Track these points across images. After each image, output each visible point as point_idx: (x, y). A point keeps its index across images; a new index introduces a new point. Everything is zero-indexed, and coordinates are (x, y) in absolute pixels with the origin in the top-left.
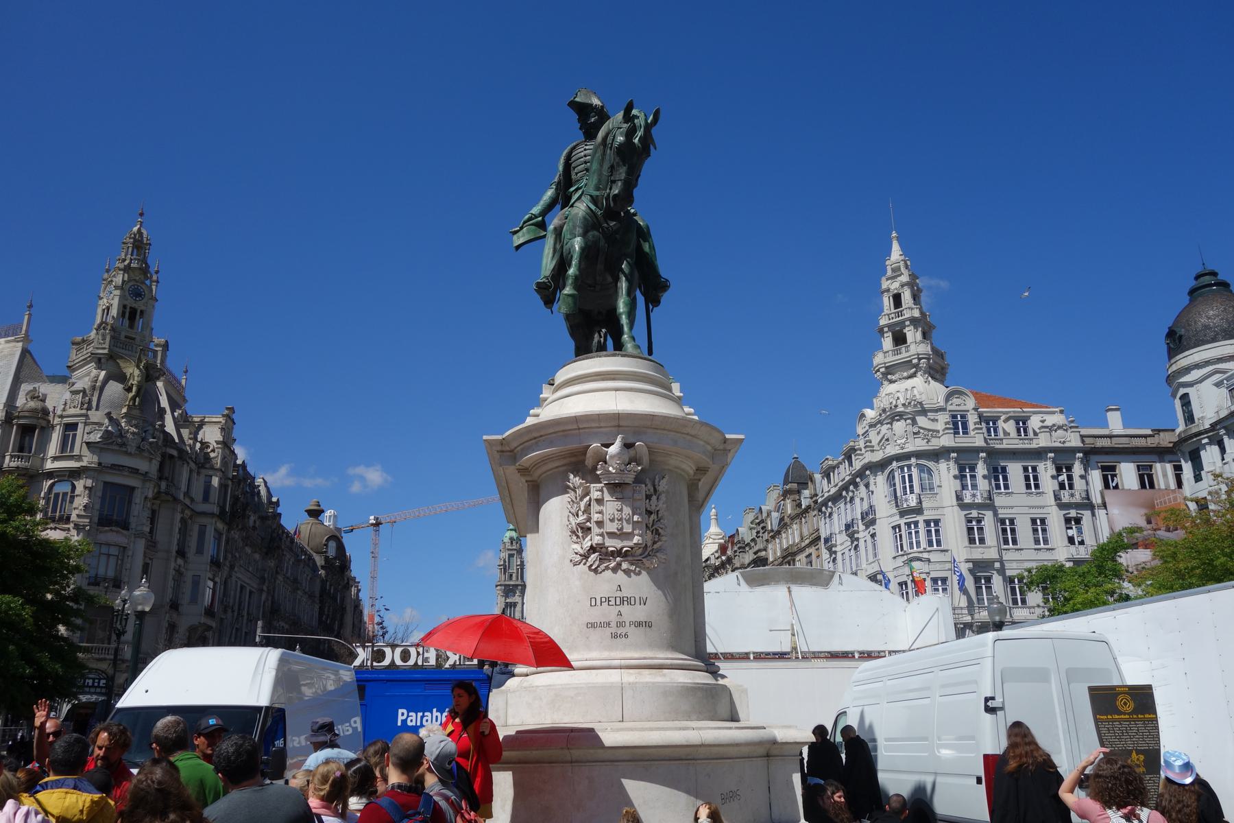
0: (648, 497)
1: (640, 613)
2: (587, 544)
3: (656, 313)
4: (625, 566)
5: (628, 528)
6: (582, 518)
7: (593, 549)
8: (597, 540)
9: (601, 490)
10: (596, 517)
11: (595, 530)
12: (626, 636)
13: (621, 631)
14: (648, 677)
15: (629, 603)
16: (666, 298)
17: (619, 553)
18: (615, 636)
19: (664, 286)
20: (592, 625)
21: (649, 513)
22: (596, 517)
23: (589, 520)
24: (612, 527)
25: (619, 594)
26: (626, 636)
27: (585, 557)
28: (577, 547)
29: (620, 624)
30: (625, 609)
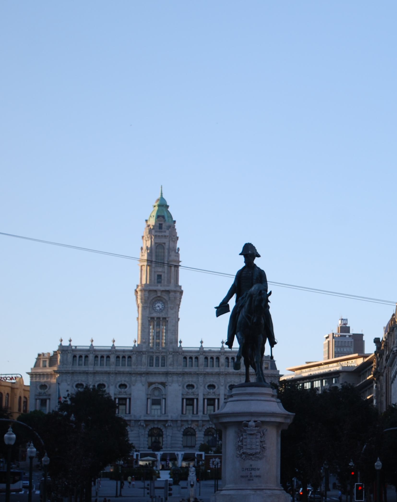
0: (261, 437)
1: (258, 473)
2: (241, 452)
3: (273, 348)
4: (253, 459)
5: (254, 447)
6: (240, 444)
7: (243, 453)
8: (245, 451)
9: (246, 435)
10: (244, 444)
11: (244, 447)
12: (253, 480)
13: (251, 478)
14: (258, 492)
15: (254, 470)
16: (275, 345)
17: (251, 455)
18: (249, 480)
19: (276, 343)
20: (242, 477)
21: (261, 442)
22: (244, 444)
23: (242, 444)
24: (249, 447)
25: (251, 467)
26: (253, 480)
27: (241, 455)
28: (238, 452)
29: (251, 476)
30: (253, 472)
